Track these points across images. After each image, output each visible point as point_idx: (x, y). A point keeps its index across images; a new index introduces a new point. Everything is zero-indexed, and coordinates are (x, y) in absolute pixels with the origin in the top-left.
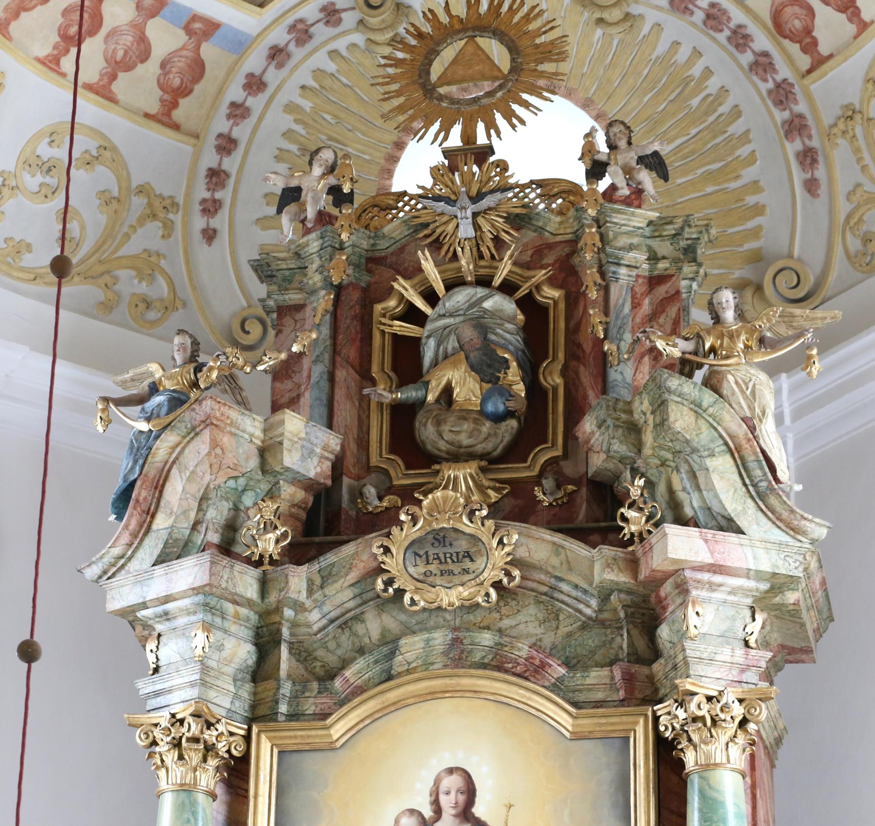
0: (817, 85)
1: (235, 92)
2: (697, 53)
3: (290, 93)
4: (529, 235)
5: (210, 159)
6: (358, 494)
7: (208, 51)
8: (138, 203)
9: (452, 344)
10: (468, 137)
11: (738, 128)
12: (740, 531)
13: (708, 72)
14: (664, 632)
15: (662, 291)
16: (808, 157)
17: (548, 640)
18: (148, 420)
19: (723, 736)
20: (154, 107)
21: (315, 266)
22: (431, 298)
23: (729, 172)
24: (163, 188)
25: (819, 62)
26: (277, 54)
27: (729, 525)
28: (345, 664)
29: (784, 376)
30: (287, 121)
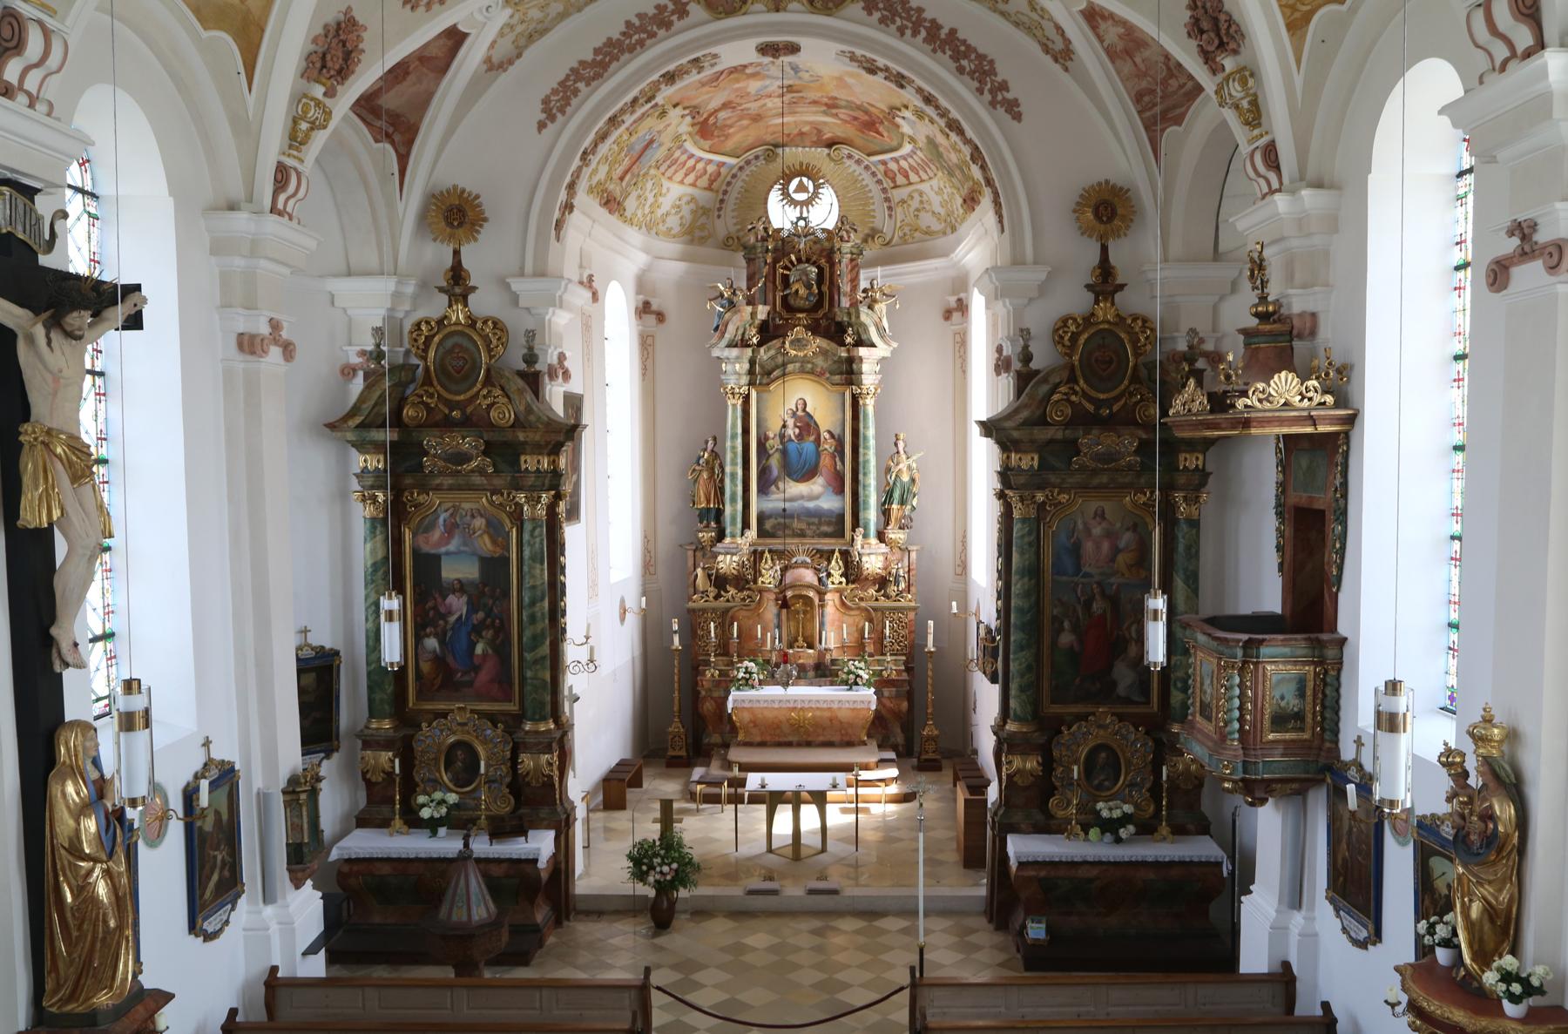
0: (894, 191)
1: (729, 179)
2: (860, 174)
3: (744, 177)
4: (818, 246)
5: (721, 197)
6: (774, 319)
7: (723, 170)
8: (700, 212)
9: (798, 277)
10: (801, 213)
11: (870, 195)
12: (875, 346)
13: (863, 180)
14: (855, 366)
15: (854, 263)
16: (890, 208)
17: (825, 366)
18: (722, 307)
19: (869, 397)
20: (707, 186)
21: (759, 250)
22: (793, 265)
23: (865, 205)
24: (708, 206)
25: (896, 187)
26: (741, 168)
27: (873, 345)
28: (773, 370)
29: (879, 268)
30: (742, 184)
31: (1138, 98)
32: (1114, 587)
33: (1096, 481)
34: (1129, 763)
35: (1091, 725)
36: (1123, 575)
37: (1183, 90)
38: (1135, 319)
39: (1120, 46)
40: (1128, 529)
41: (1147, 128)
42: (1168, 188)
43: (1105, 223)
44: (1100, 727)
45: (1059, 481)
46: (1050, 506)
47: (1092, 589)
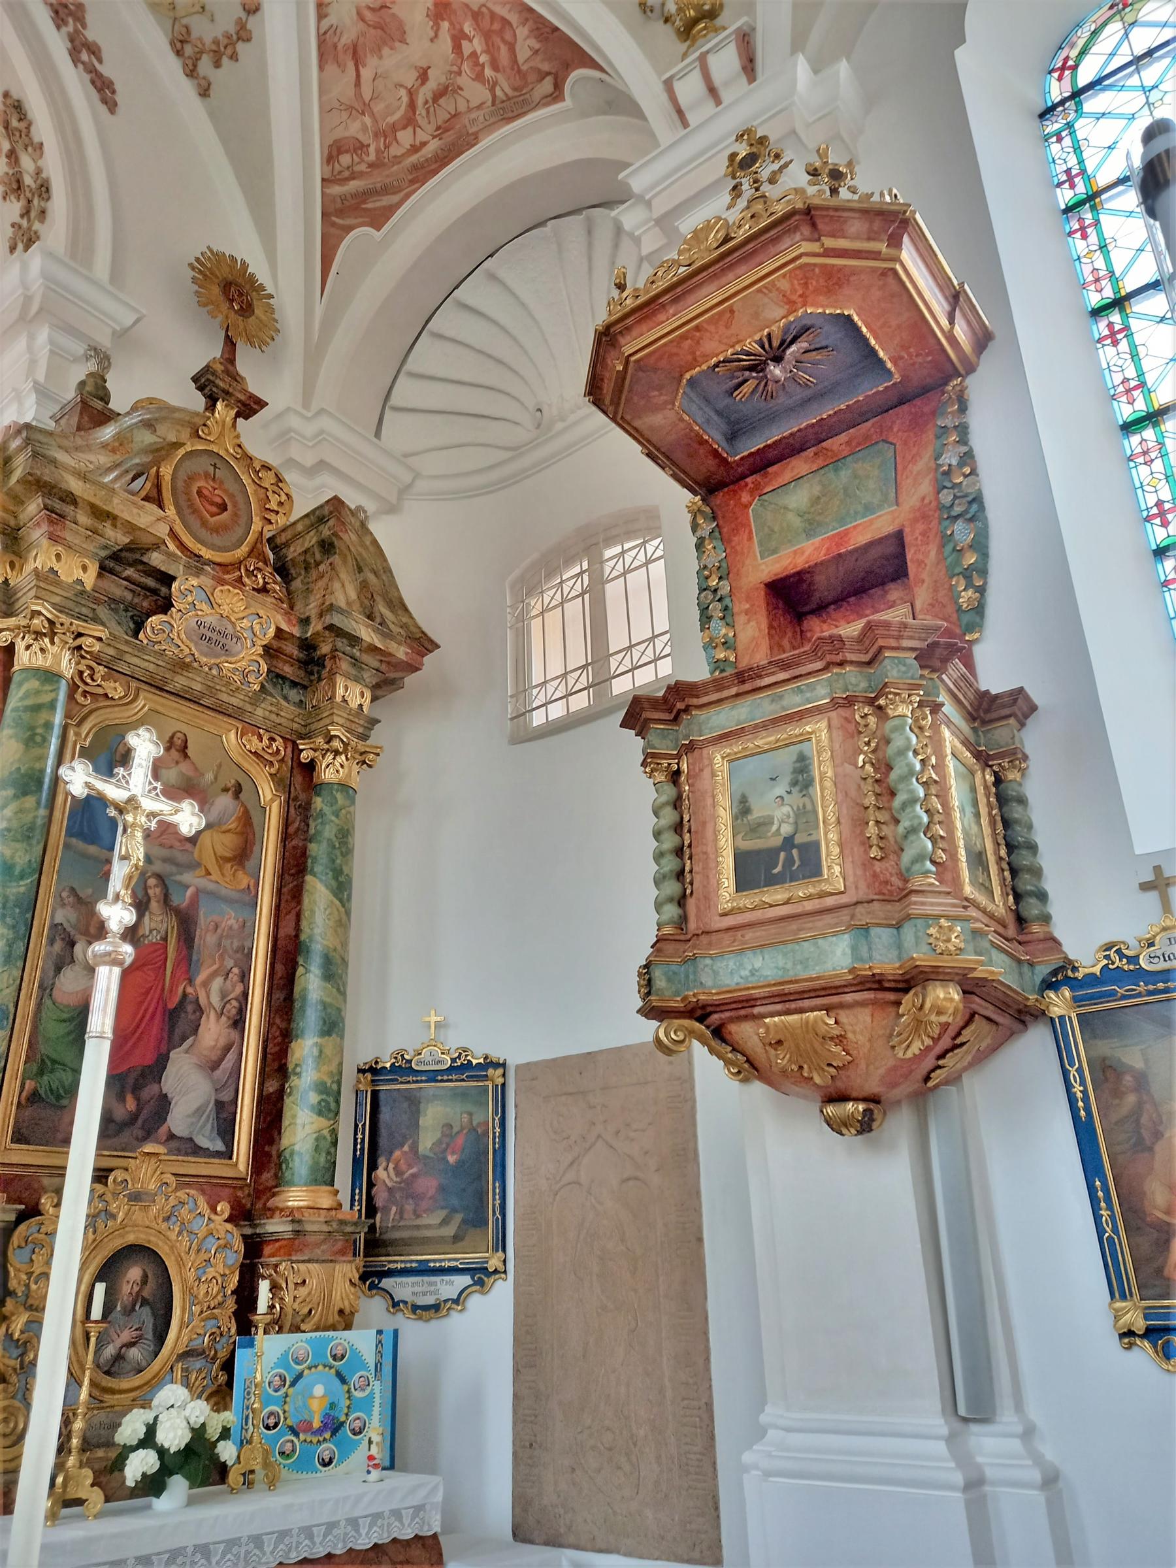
31: (333, 153)
32: (189, 892)
33: (179, 682)
34: (189, 1292)
35: (116, 1195)
36: (208, 873)
37: (413, 159)
38: (266, 467)
39: (346, 39)
40: (226, 790)
41: (324, 215)
42: (330, 324)
43: (236, 312)
44: (135, 1197)
45: (111, 652)
46: (85, 693)
47: (146, 888)
